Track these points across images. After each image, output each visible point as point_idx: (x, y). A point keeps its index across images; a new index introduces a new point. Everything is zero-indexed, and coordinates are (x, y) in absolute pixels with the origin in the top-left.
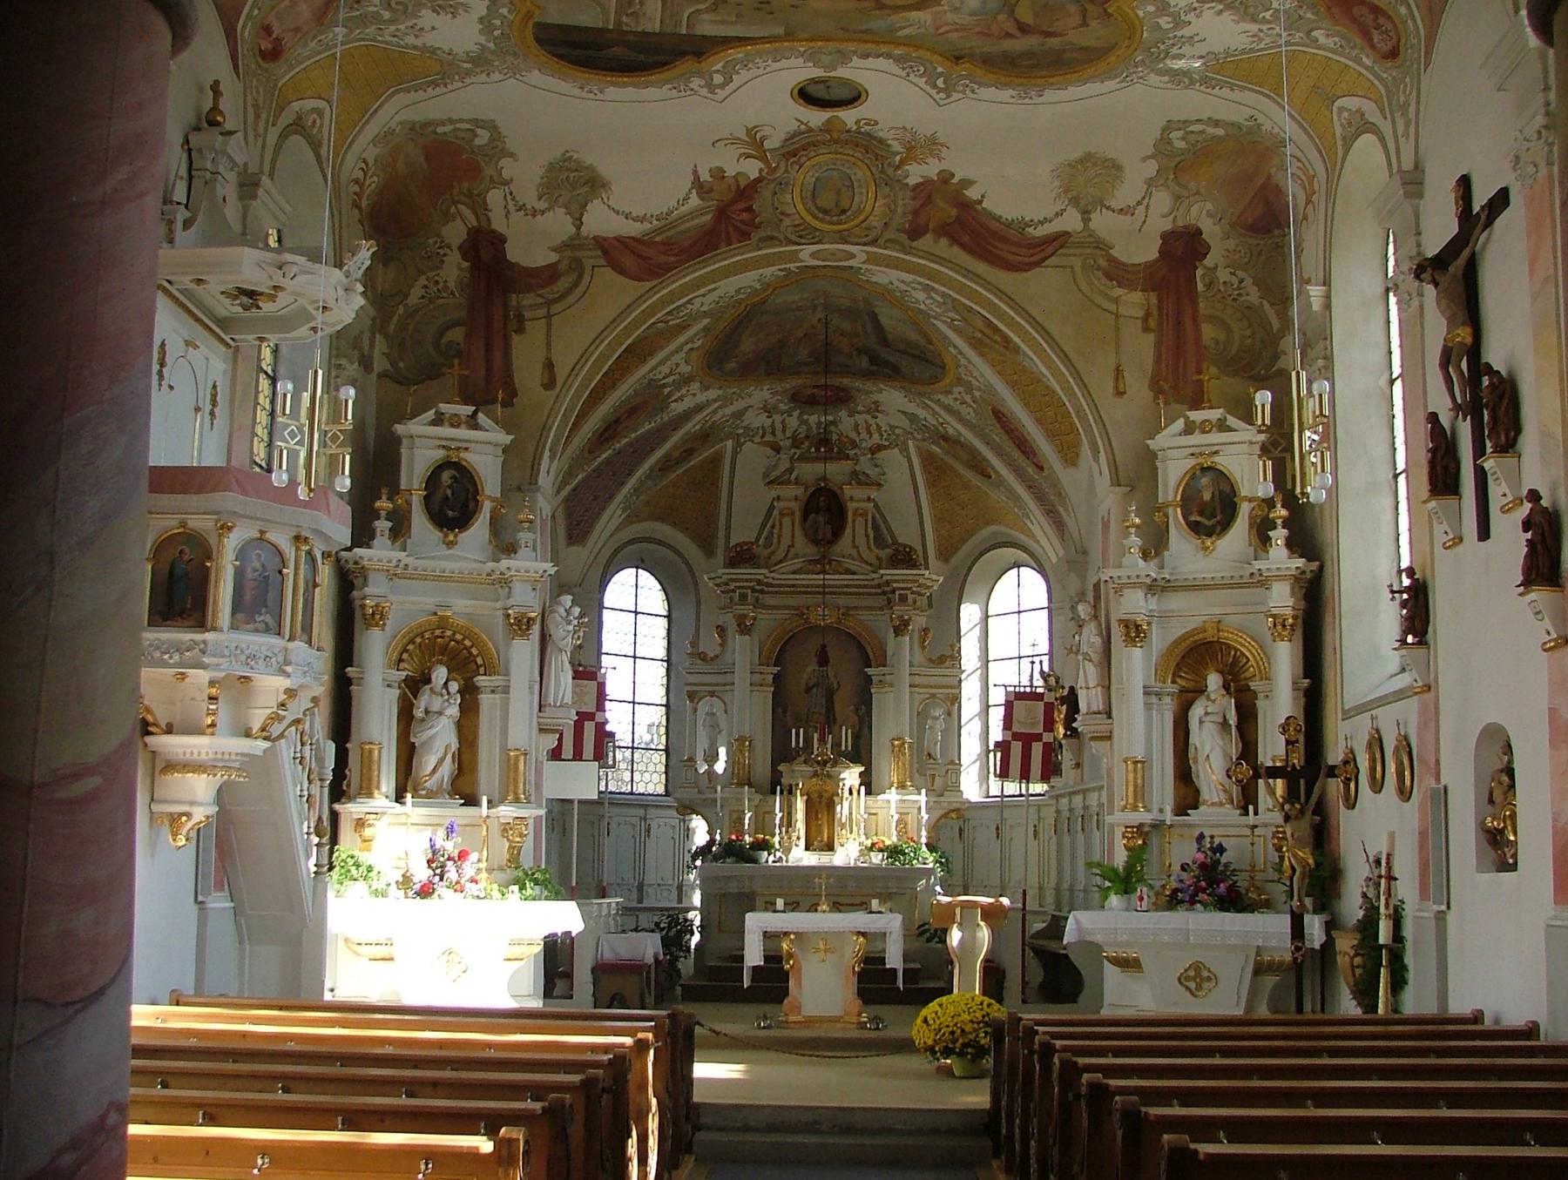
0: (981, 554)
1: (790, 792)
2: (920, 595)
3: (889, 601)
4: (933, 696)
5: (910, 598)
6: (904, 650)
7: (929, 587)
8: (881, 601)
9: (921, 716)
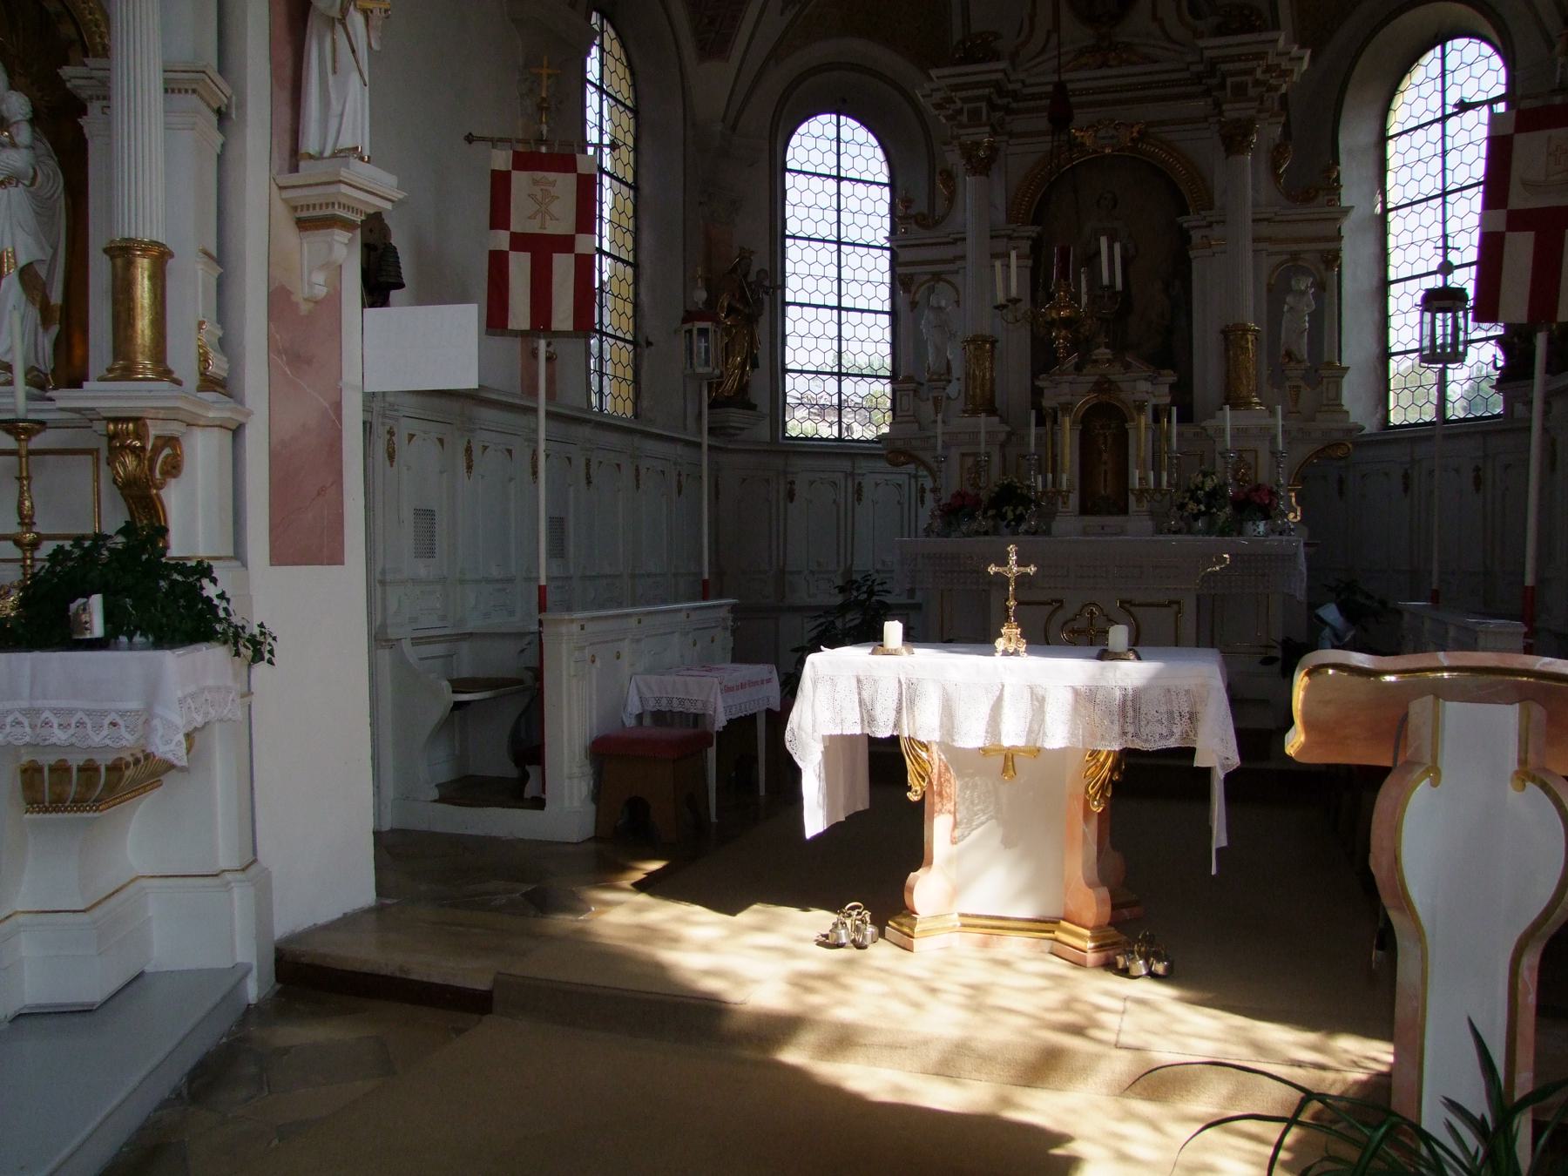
0: (1375, 31)
1: (1055, 421)
2: (1271, 89)
3: (1218, 105)
4: (1295, 256)
5: (1252, 92)
6: (1246, 184)
7: (1285, 74)
8: (1199, 106)
9: (1277, 293)
